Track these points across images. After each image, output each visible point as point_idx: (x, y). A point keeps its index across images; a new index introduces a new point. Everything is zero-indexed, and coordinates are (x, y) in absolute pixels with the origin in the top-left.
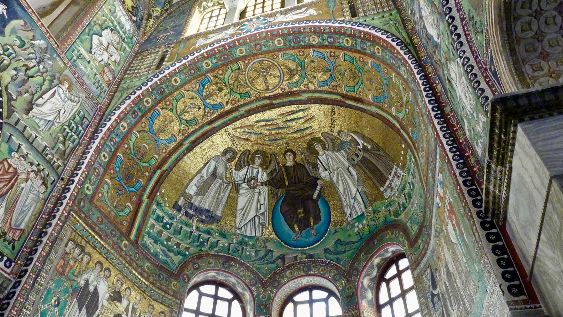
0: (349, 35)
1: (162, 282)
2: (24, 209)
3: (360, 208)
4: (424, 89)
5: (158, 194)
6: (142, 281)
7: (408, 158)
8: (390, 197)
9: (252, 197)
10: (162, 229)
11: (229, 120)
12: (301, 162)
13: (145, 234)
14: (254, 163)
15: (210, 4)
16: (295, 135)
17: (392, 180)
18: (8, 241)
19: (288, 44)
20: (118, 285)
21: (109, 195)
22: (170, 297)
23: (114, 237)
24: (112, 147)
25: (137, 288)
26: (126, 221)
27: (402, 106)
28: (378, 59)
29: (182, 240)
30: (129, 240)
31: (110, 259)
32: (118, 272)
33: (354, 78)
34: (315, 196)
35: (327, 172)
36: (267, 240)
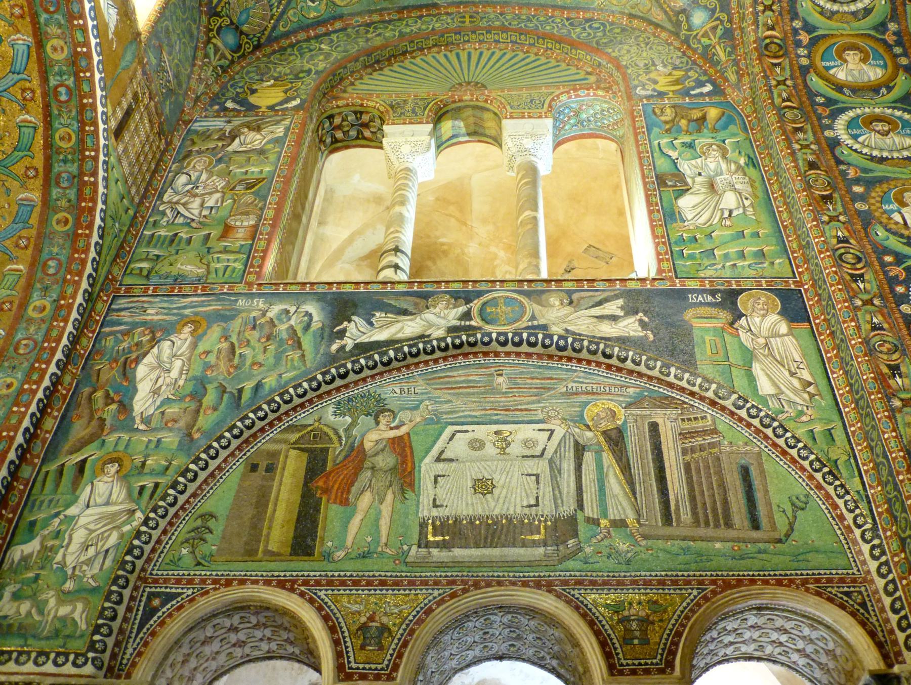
28: (44, 220)
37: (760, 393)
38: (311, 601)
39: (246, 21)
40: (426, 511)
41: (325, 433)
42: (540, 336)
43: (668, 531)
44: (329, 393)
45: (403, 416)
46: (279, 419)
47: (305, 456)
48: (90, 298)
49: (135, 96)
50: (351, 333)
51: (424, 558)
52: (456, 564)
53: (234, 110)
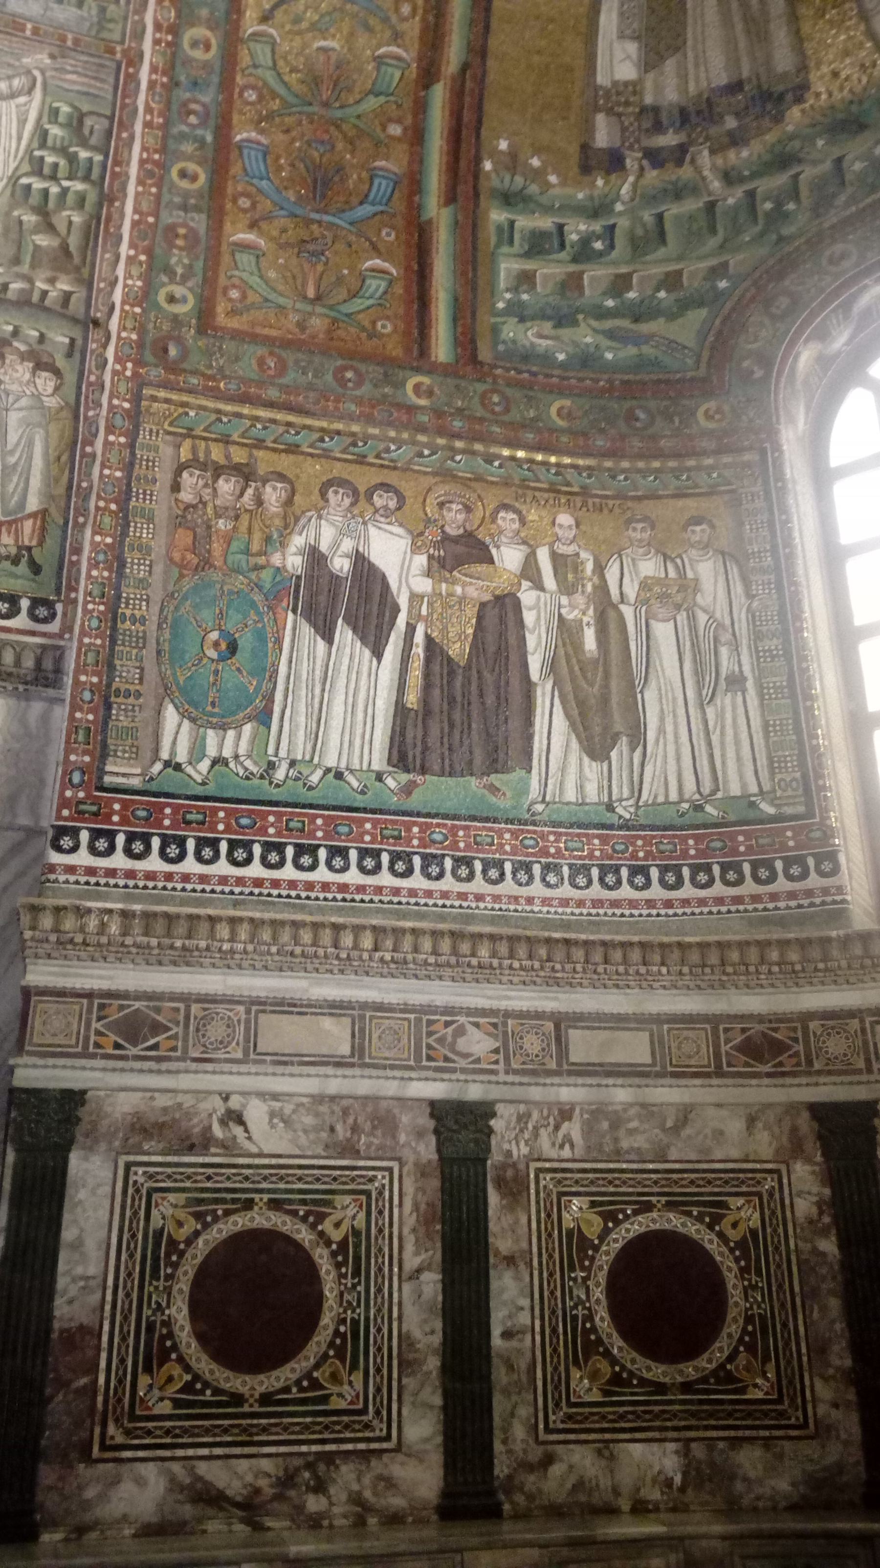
1: (650, 431)
2: (12, 460)
5: (488, 166)
6: (558, 465)
10: (573, 268)
13: (499, 320)
18: (7, 558)
20: (449, 516)
21: (272, 274)
22: (709, 461)
23: (359, 383)
24: (199, 132)
25: (546, 495)
26: (388, 318)
29: (680, 258)
30: (433, 369)
31: (378, 456)
32: (433, 480)
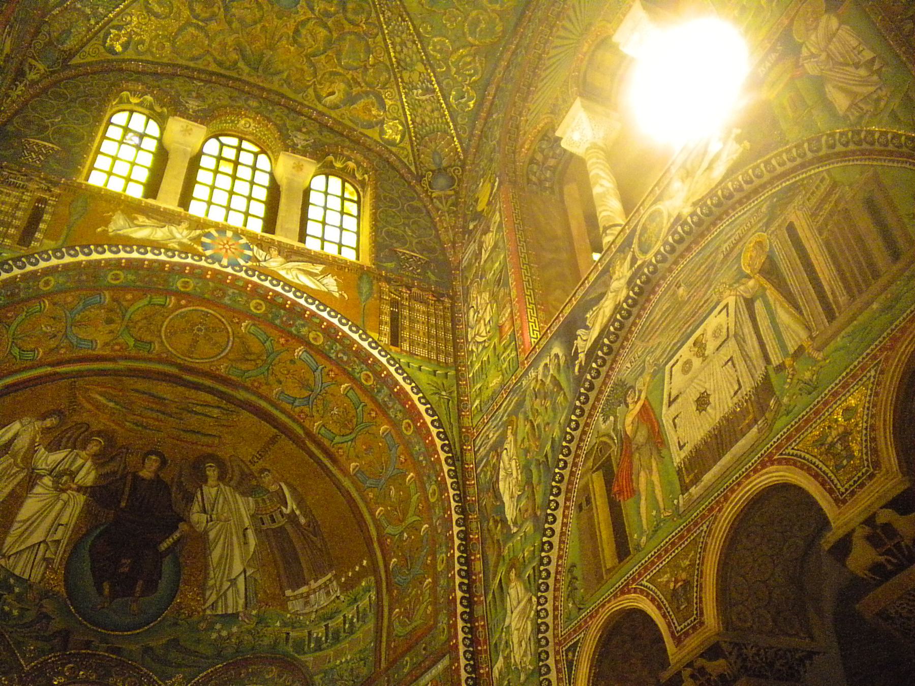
0: (377, 374)
3: (235, 602)
4: (459, 558)
7: (363, 584)
8: (296, 614)
9: (53, 505)
11: (89, 371)
12: (167, 480)
14: (85, 449)
15: (134, 100)
16: (184, 435)
17: (314, 591)
19: (270, 316)
27: (402, 521)
33: (345, 426)
34: (164, 546)
35: (204, 516)
36: (46, 594)
37: (841, 113)
38: (642, 592)
39: (441, 159)
40: (678, 457)
41: (605, 443)
42: (679, 229)
43: (835, 324)
44: (594, 407)
45: (639, 385)
46: (577, 456)
47: (600, 473)
48: (457, 459)
49: (394, 303)
50: (582, 348)
51: (690, 500)
52: (709, 490)
53: (475, 227)
